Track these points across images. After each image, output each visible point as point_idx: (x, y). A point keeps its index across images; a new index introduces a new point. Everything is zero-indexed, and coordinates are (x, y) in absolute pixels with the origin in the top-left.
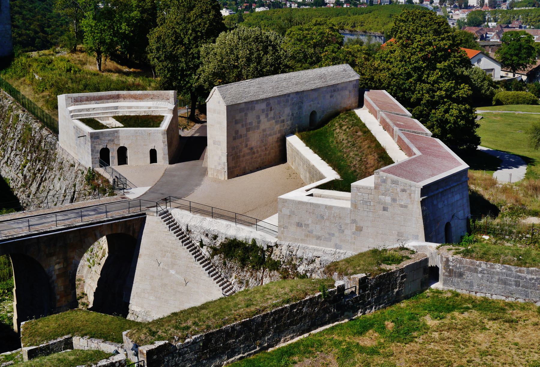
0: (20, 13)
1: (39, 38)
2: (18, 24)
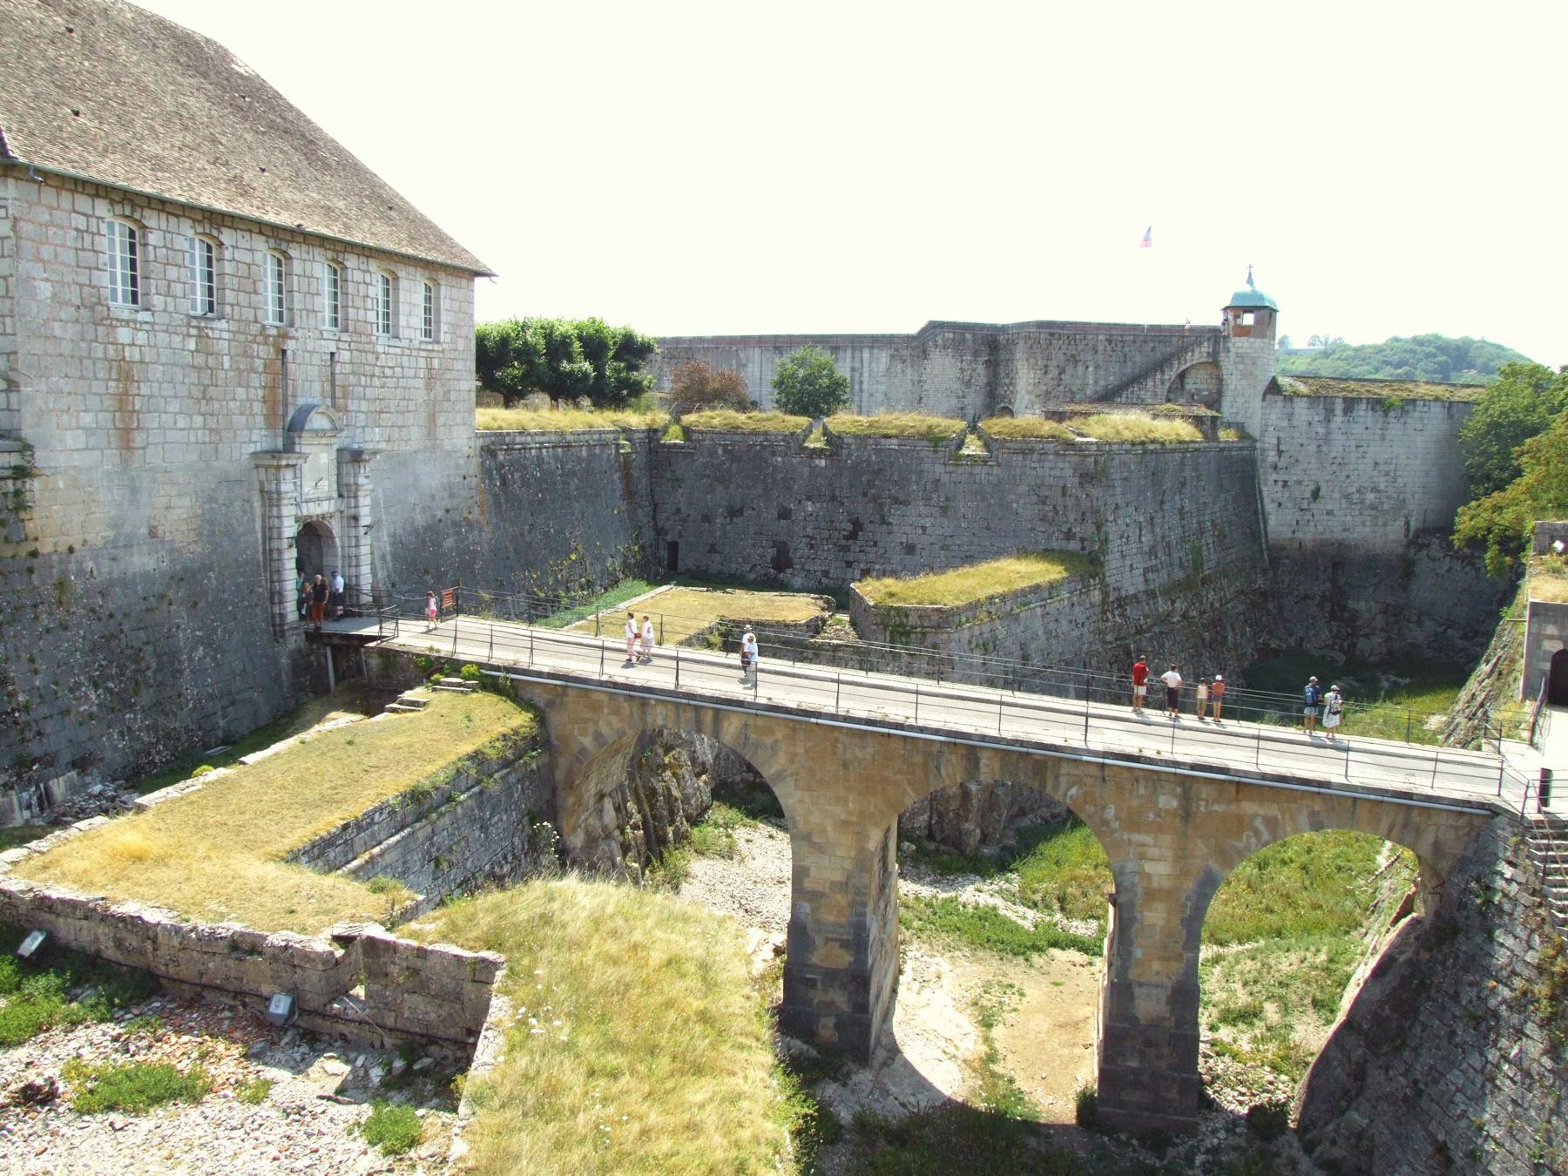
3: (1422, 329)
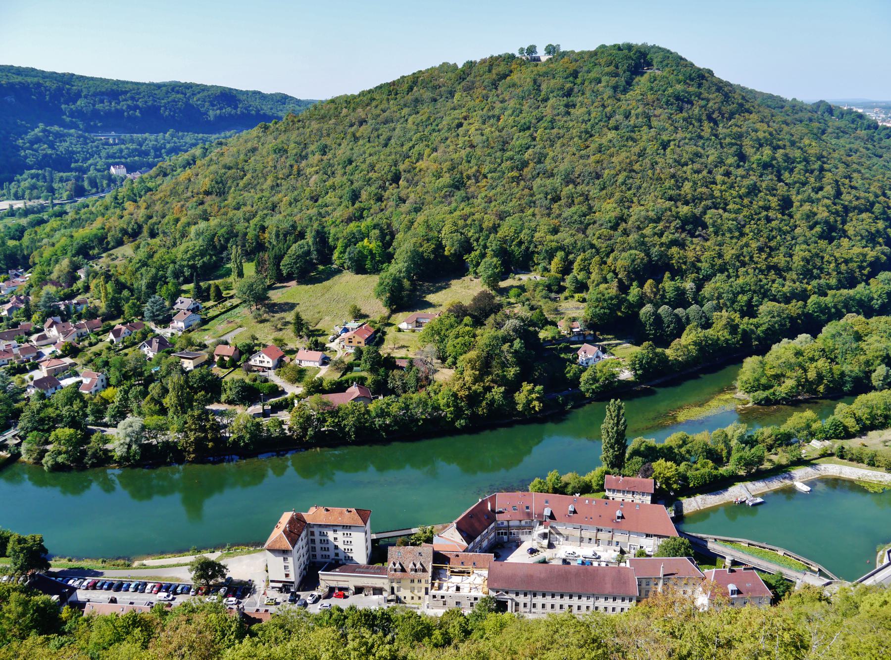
0: (859, 172)
1: (879, 203)
2: (857, 185)
3: (620, 42)
